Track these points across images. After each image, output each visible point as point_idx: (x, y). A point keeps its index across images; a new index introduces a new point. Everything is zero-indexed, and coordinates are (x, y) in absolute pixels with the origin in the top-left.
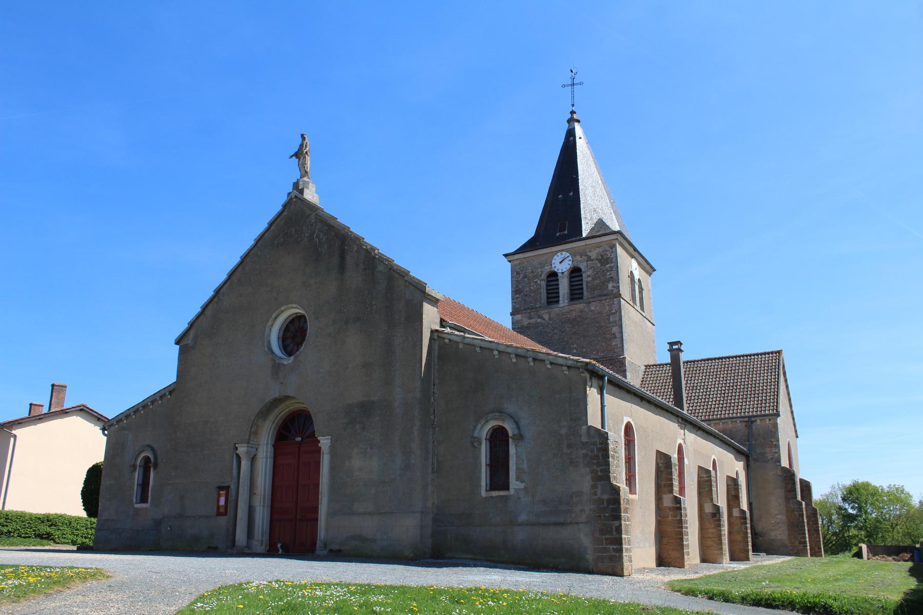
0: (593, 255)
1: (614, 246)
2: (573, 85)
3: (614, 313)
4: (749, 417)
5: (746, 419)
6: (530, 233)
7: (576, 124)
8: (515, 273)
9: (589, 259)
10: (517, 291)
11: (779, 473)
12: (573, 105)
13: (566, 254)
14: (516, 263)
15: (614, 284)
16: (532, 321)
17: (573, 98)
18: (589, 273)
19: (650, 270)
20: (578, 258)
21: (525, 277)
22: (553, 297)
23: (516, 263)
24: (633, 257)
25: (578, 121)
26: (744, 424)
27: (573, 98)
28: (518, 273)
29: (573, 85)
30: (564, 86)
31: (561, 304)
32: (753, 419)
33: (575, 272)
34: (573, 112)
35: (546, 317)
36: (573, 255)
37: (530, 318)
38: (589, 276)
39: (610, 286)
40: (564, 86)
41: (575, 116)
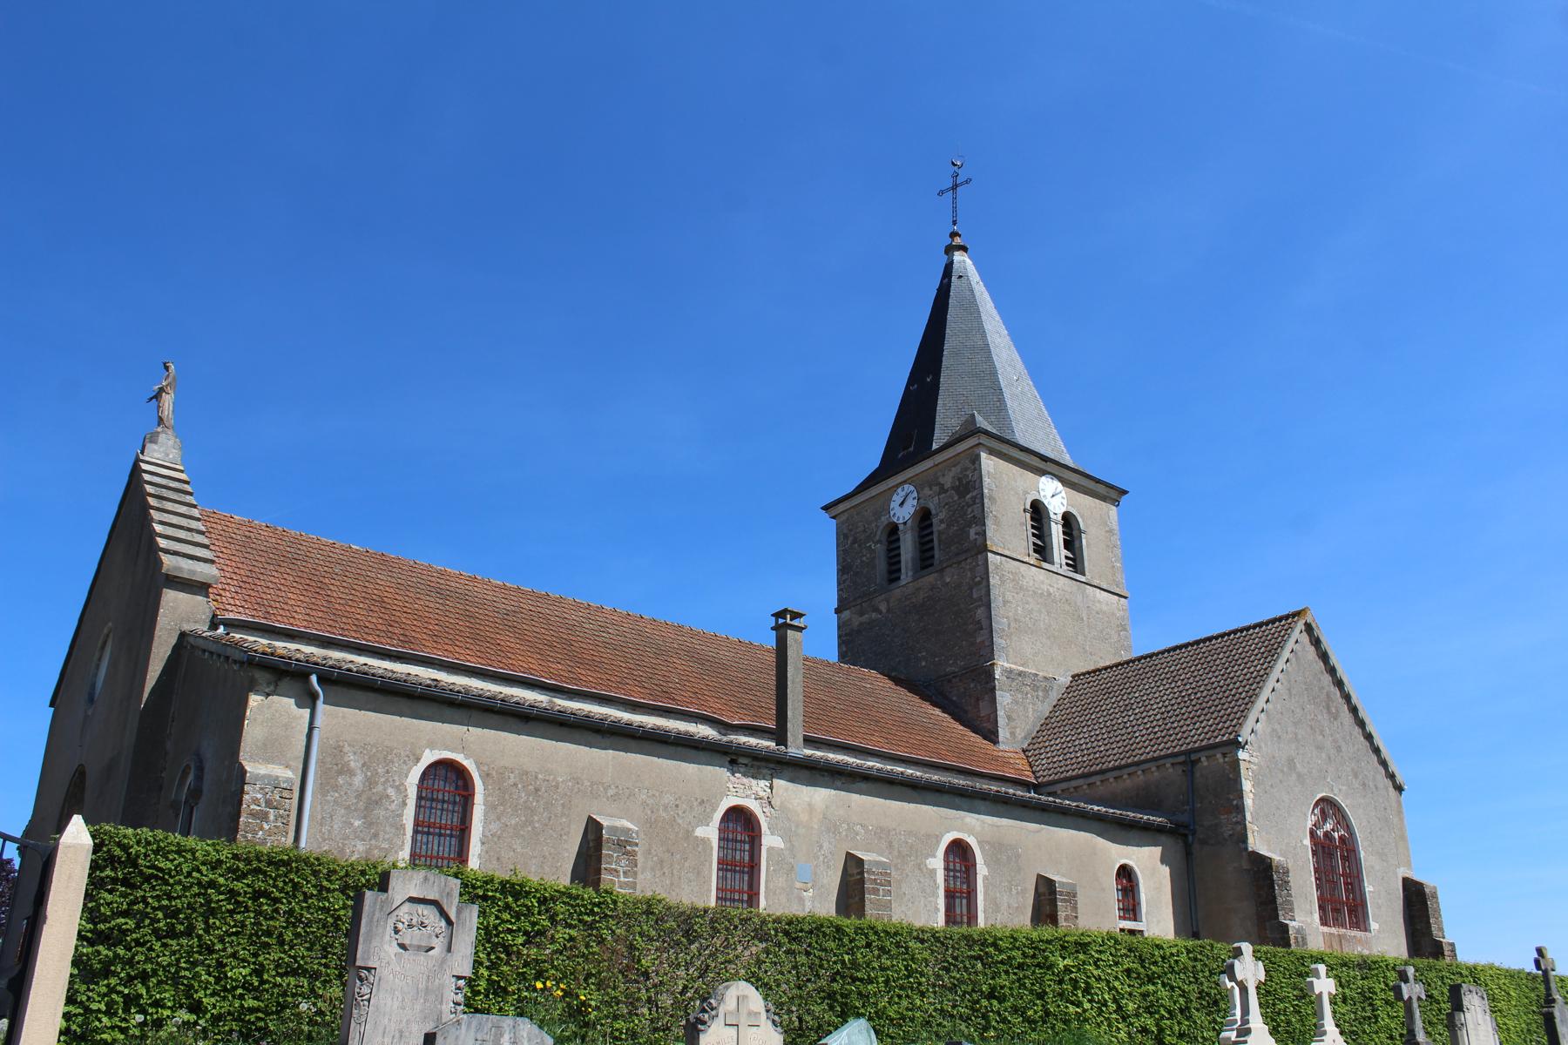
0: (947, 481)
1: (978, 456)
2: (955, 187)
3: (979, 583)
4: (1188, 753)
5: (1182, 759)
6: (875, 463)
7: (958, 257)
8: (842, 536)
9: (943, 490)
10: (844, 569)
11: (1245, 865)
12: (954, 223)
13: (908, 488)
14: (844, 517)
15: (978, 528)
16: (865, 618)
17: (955, 209)
18: (941, 516)
19: (1113, 494)
20: (927, 491)
21: (854, 542)
22: (894, 573)
23: (844, 517)
24: (1042, 473)
25: (964, 249)
26: (1179, 769)
27: (955, 209)
28: (846, 537)
29: (955, 187)
30: (941, 193)
31: (903, 582)
32: (1193, 757)
33: (924, 517)
34: (954, 235)
35: (883, 607)
36: (919, 489)
37: (862, 614)
38: (942, 521)
39: (972, 532)
40: (941, 193)
41: (958, 241)
